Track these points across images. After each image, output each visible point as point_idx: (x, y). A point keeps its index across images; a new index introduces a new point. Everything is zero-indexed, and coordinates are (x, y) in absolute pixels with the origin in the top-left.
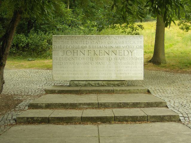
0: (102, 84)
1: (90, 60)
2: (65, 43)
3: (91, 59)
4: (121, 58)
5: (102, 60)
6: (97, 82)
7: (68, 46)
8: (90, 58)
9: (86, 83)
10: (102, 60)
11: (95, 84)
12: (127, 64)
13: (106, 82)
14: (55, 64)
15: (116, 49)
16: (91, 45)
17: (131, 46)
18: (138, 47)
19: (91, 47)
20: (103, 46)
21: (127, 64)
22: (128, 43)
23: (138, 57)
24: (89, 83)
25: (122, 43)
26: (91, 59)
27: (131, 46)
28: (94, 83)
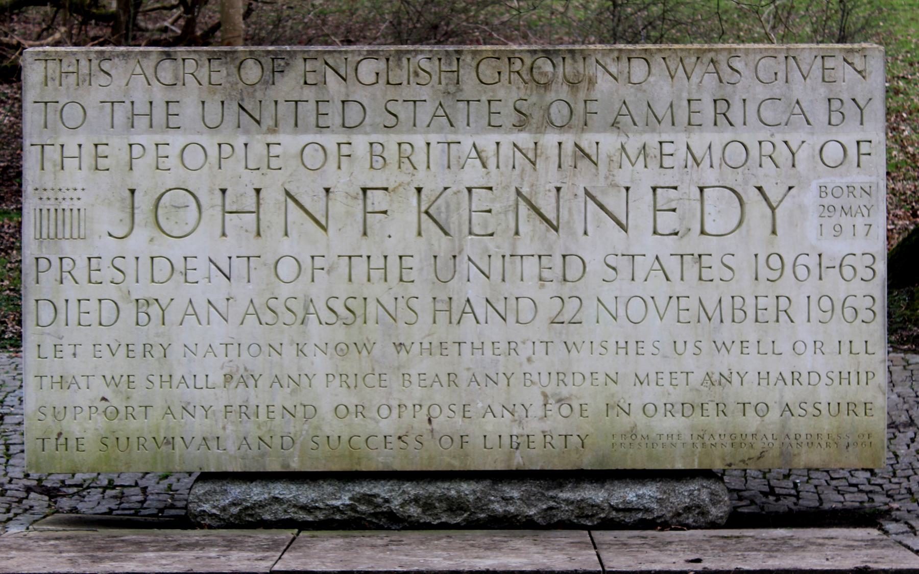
0: (498, 508)
1: (376, 275)
2: (142, 122)
3: (393, 262)
4: (672, 265)
5: (496, 275)
6: (437, 489)
7: (173, 151)
8: (377, 262)
9: (343, 498)
10: (496, 275)
11: (427, 505)
12: (727, 318)
13: (532, 487)
14: (46, 314)
15: (623, 177)
16: (391, 138)
17: (767, 148)
18: (833, 153)
19: (392, 152)
20: (506, 149)
21: (727, 318)
22: (736, 114)
23: (836, 248)
24: (368, 499)
25: (682, 115)
26: (393, 262)
27: (767, 148)
28: (416, 500)
